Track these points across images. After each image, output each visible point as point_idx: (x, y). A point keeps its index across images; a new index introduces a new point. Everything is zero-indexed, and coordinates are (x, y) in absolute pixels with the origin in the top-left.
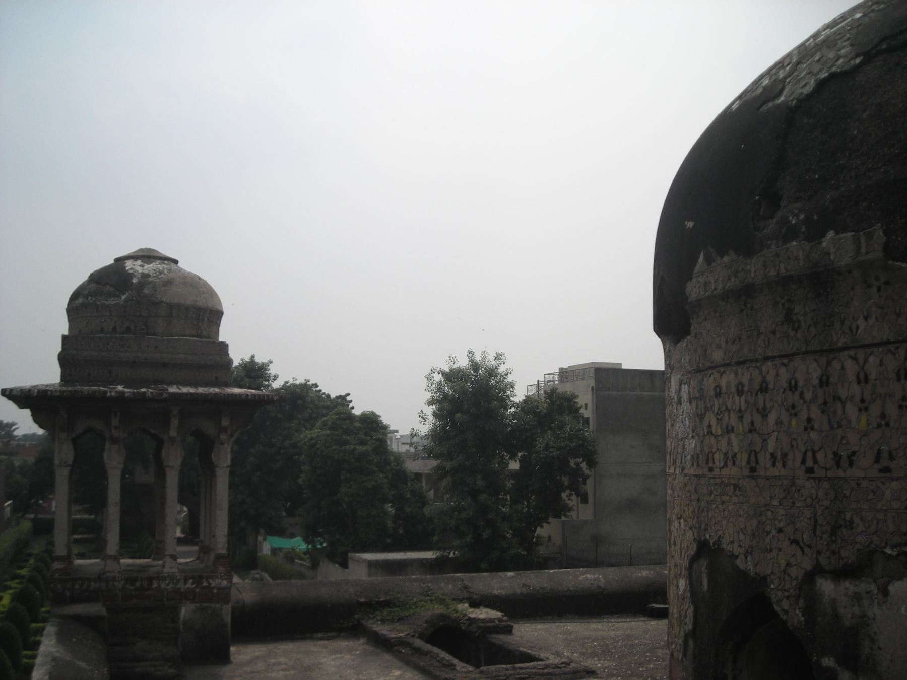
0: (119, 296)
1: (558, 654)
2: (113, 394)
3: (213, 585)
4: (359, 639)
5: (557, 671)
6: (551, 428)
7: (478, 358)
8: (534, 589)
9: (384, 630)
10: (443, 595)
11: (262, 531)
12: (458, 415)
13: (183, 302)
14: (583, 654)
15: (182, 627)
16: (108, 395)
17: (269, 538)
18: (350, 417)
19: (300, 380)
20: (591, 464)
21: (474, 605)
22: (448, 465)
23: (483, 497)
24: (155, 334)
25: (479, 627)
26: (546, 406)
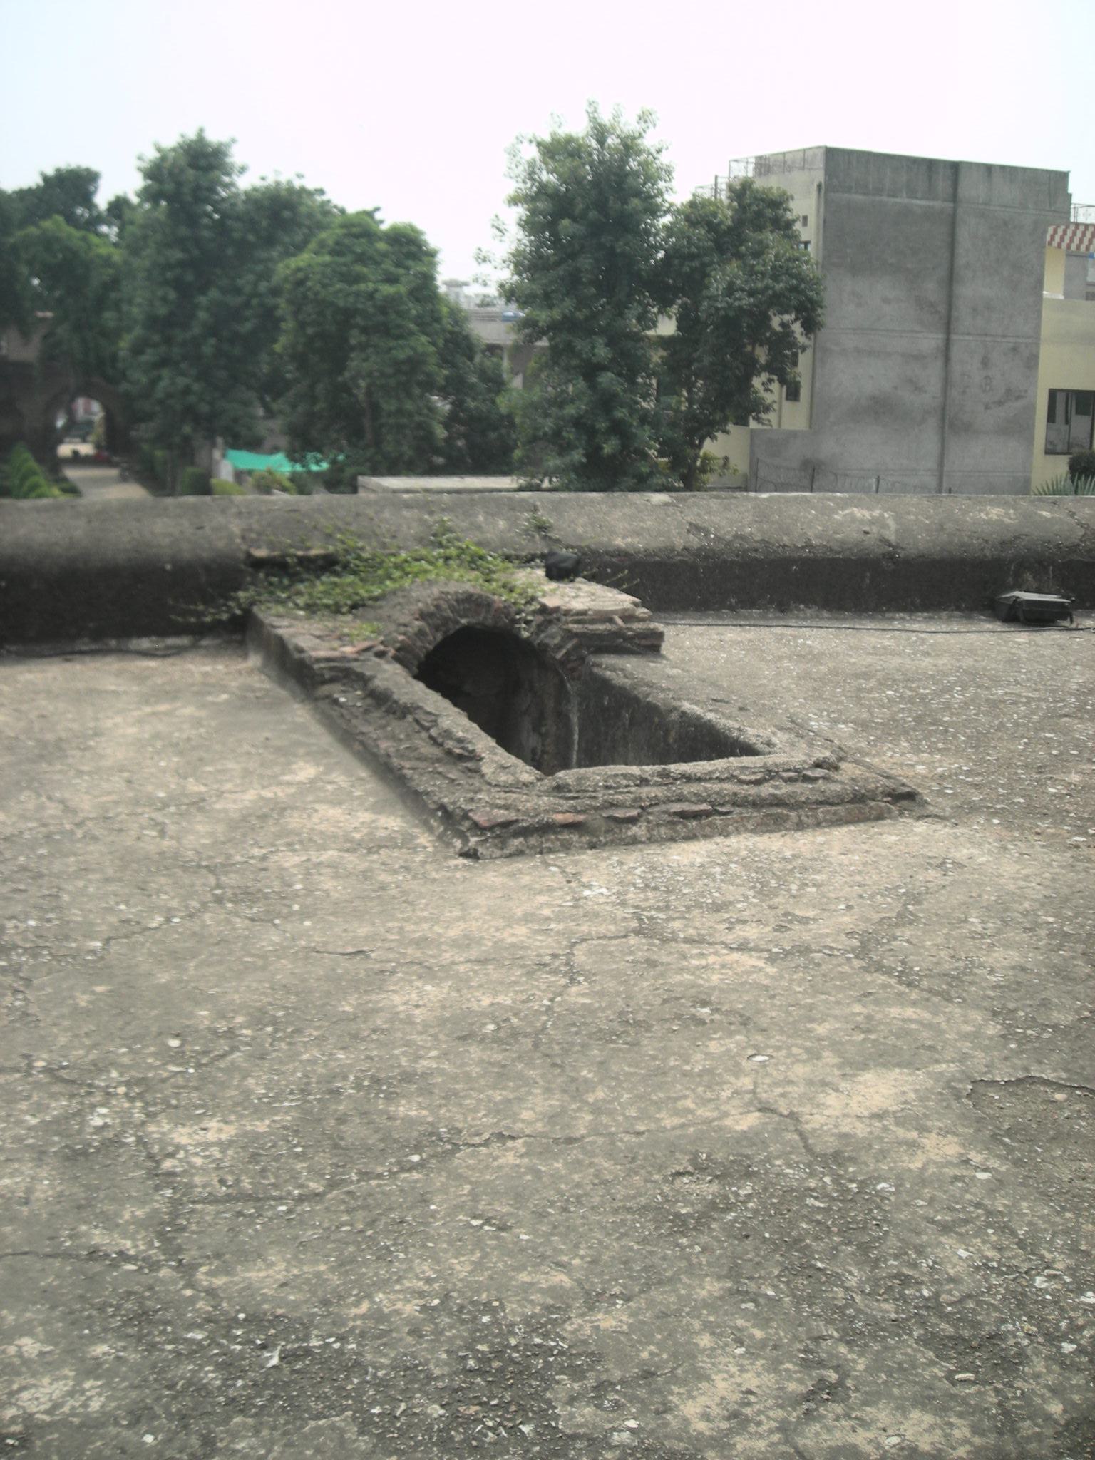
1: (797, 728)
4: (245, 657)
5: (802, 790)
6: (739, 256)
7: (605, 118)
8: (718, 539)
9: (307, 635)
10: (479, 544)
11: (220, 440)
12: (566, 222)
14: (864, 726)
17: (233, 454)
20: (811, 326)
21: (559, 572)
22: (543, 316)
23: (606, 379)
25: (570, 635)
26: (730, 213)
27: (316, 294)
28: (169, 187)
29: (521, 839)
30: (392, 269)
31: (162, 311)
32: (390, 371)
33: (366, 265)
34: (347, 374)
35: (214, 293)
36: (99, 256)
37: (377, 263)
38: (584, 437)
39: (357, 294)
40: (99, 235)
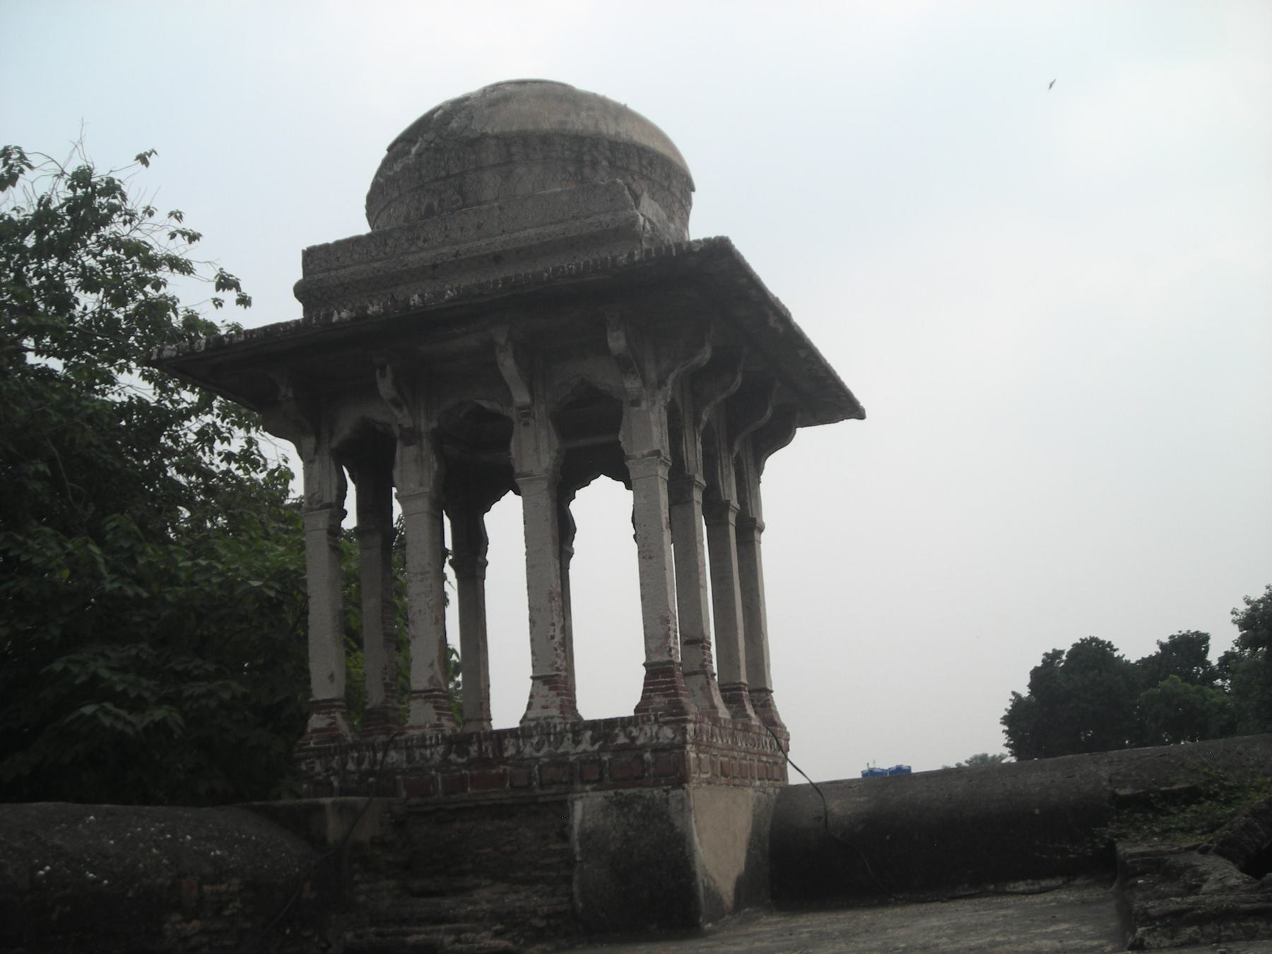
0: (409, 152)
2: (344, 314)
3: (640, 741)
13: (531, 127)
15: (577, 848)
16: (335, 318)
19: (623, 103)
24: (479, 203)
29: (1195, 928)
40: (1214, 687)
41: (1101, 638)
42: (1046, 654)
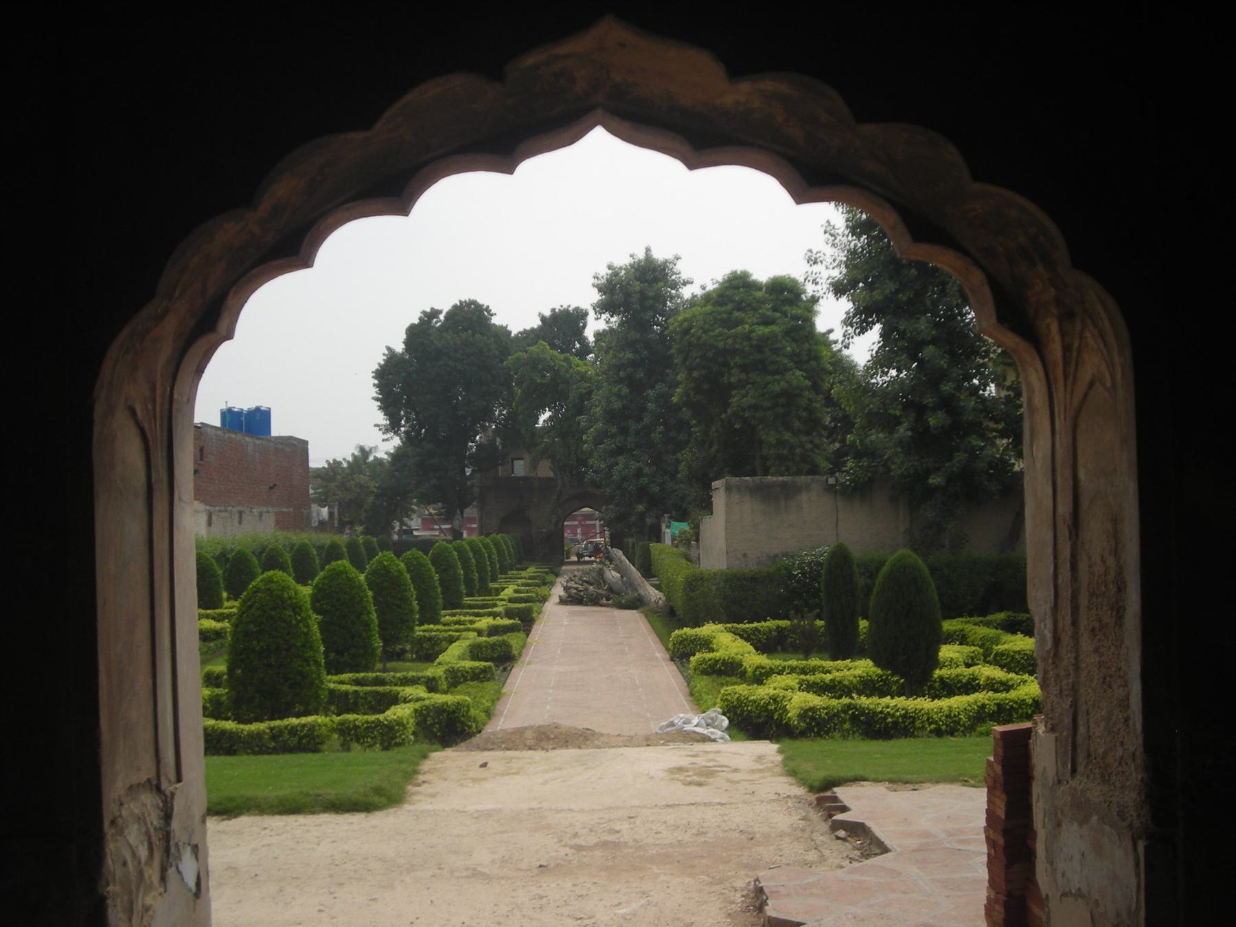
18: (755, 286)
23: (928, 352)
27: (699, 338)
28: (619, 297)
30: (769, 313)
31: (617, 405)
32: (767, 404)
33: (745, 312)
34: (729, 411)
35: (660, 387)
36: (578, 373)
37: (755, 309)
38: (913, 415)
39: (735, 336)
41: (481, 302)
42: (424, 312)
